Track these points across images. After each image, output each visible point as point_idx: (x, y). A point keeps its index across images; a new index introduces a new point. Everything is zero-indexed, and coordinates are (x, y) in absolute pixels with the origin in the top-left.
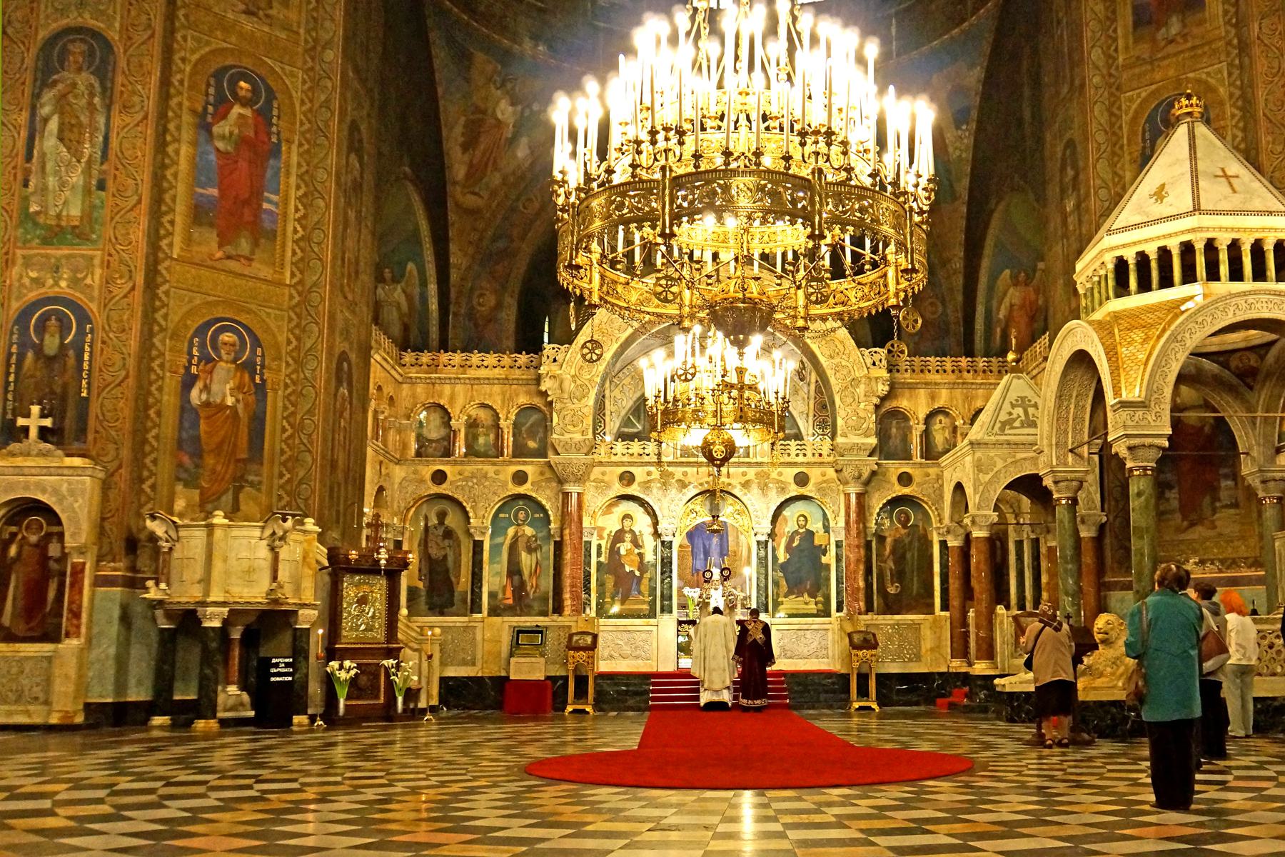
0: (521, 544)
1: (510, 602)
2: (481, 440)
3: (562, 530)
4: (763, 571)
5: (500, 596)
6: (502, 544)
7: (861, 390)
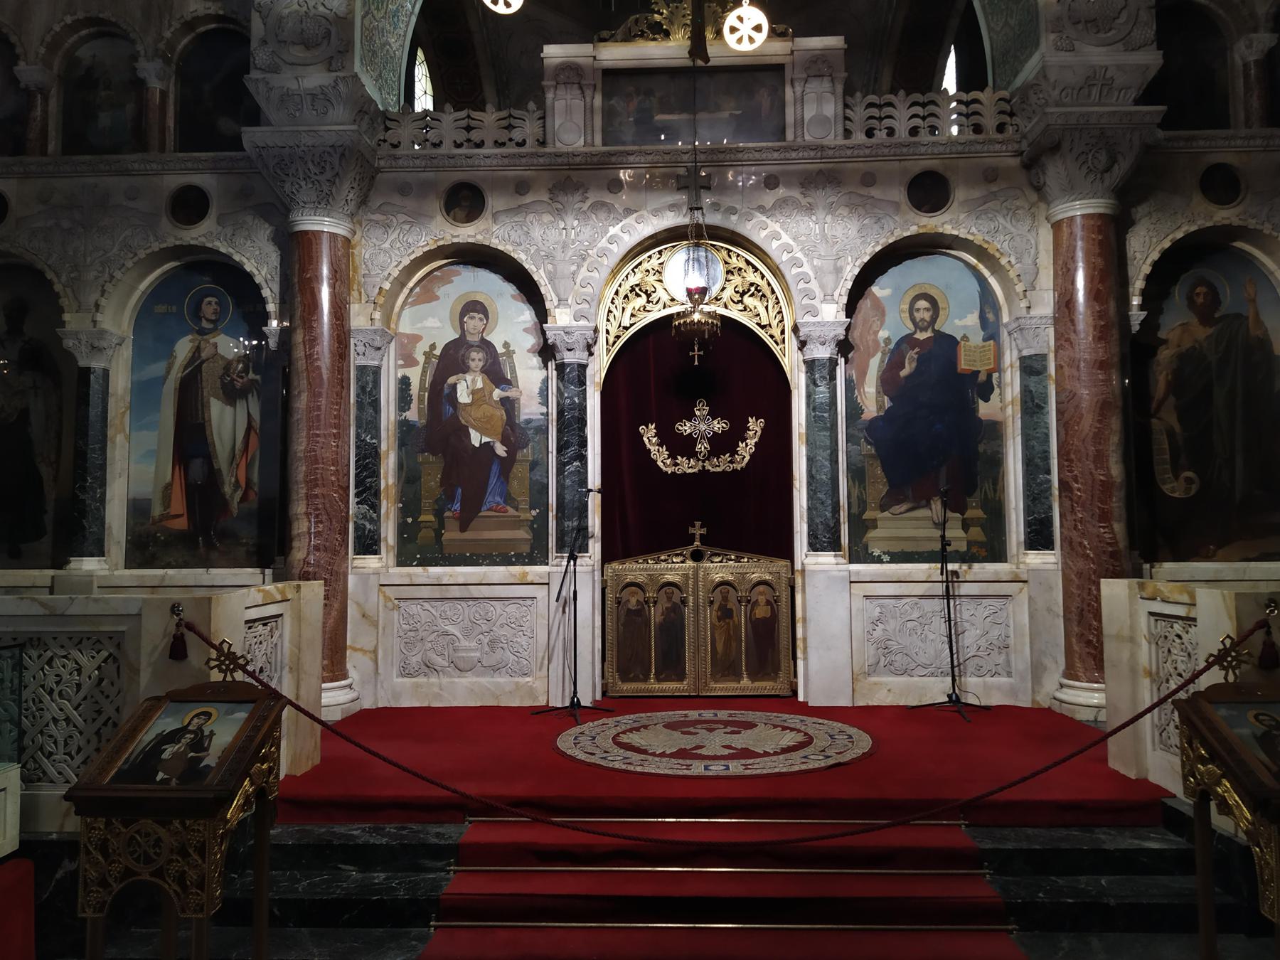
0: (210, 375)
1: (181, 524)
4: (824, 437)
5: (157, 511)
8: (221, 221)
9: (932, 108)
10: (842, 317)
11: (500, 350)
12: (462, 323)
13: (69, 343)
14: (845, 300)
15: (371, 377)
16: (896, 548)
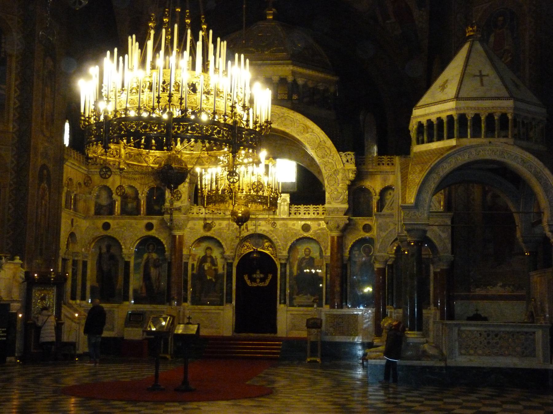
2: (130, 205)
3: (171, 255)
5: (139, 292)
6: (141, 263)
7: (340, 176)
8: (156, 230)
9: (308, 209)
10: (287, 254)
11: (214, 258)
12: (206, 252)
13: (124, 256)
14: (287, 251)
15: (186, 264)
16: (300, 304)
